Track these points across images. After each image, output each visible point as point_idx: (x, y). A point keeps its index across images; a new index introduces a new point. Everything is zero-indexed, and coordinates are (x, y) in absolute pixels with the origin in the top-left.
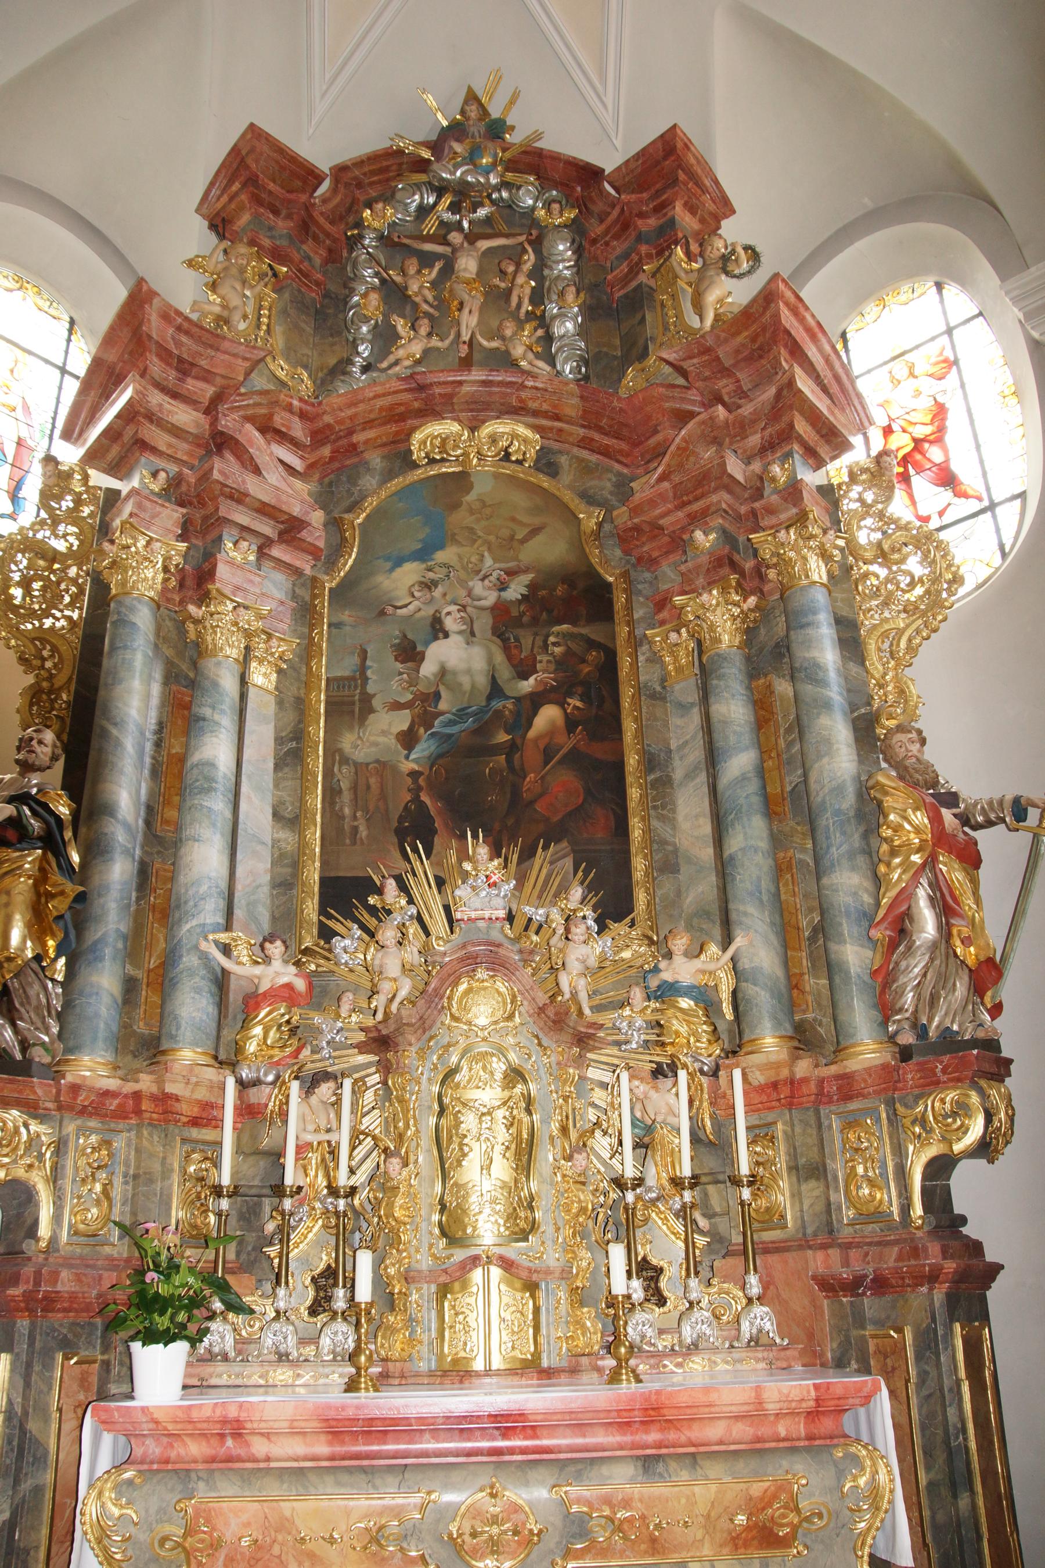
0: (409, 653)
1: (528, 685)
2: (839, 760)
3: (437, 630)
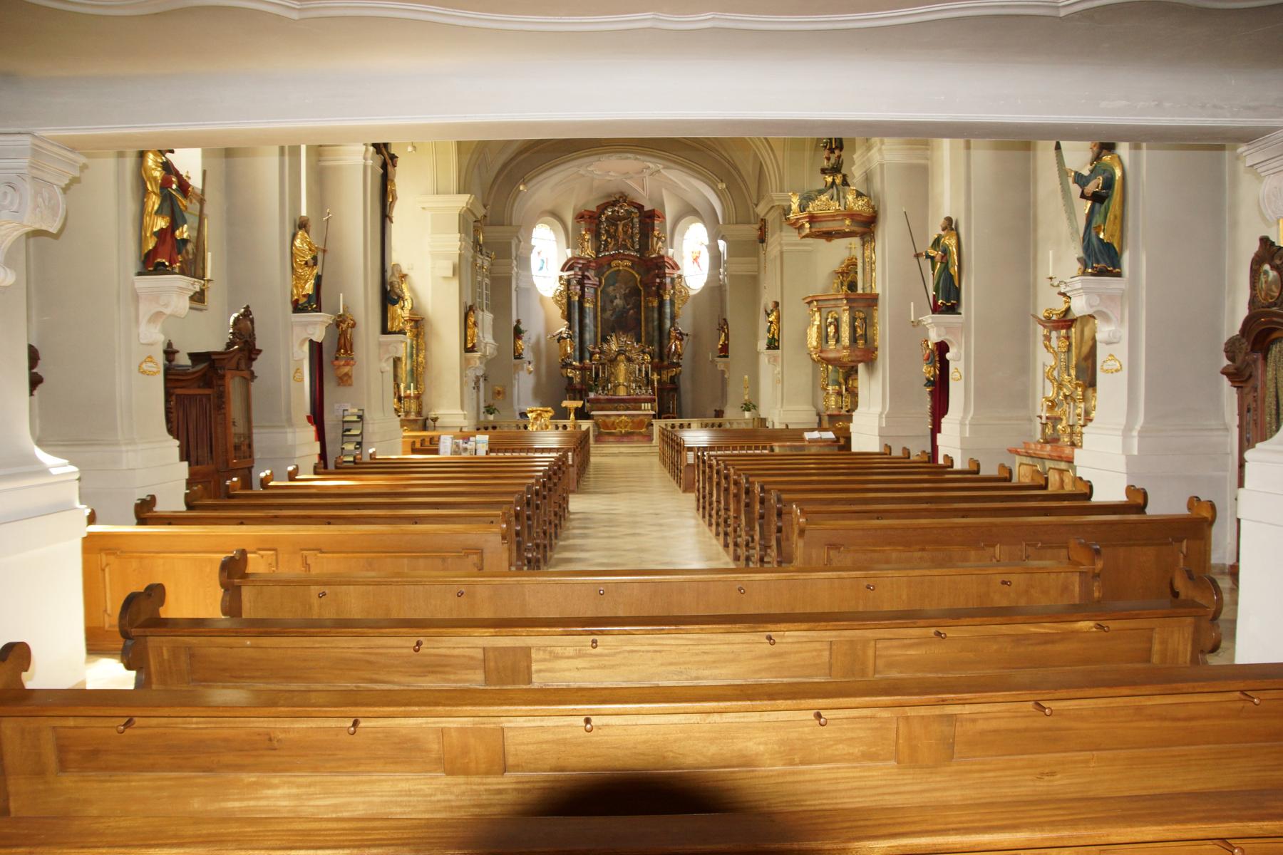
0: (612, 302)
2: (668, 324)
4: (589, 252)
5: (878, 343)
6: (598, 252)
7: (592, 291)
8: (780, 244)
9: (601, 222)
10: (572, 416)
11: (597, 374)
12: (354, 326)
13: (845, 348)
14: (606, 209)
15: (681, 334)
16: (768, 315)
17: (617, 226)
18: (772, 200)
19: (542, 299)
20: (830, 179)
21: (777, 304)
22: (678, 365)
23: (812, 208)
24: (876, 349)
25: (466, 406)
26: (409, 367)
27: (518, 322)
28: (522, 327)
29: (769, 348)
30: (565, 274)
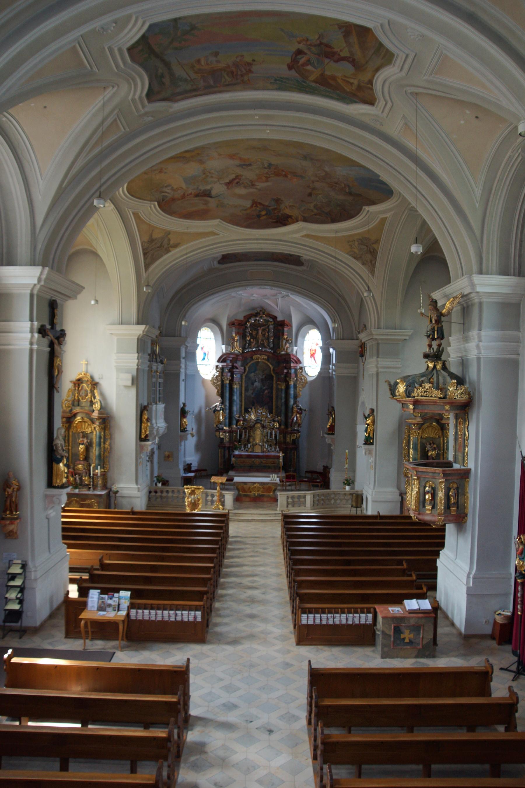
0: (253, 384)
1: (265, 388)
2: (292, 402)
3: (255, 381)
4: (238, 349)
5: (470, 510)
6: (244, 348)
7: (239, 376)
8: (377, 367)
9: (246, 327)
10: (218, 488)
11: (241, 435)
12: (19, 489)
13: (440, 515)
14: (250, 318)
15: (301, 409)
16: (366, 418)
17: (258, 330)
18: (372, 334)
19: (203, 381)
20: (431, 365)
21: (372, 411)
22: (298, 431)
23: (417, 393)
24: (466, 515)
25: (140, 481)
26: (97, 453)
27: (184, 405)
28: (187, 409)
29: (366, 444)
30: (220, 365)
